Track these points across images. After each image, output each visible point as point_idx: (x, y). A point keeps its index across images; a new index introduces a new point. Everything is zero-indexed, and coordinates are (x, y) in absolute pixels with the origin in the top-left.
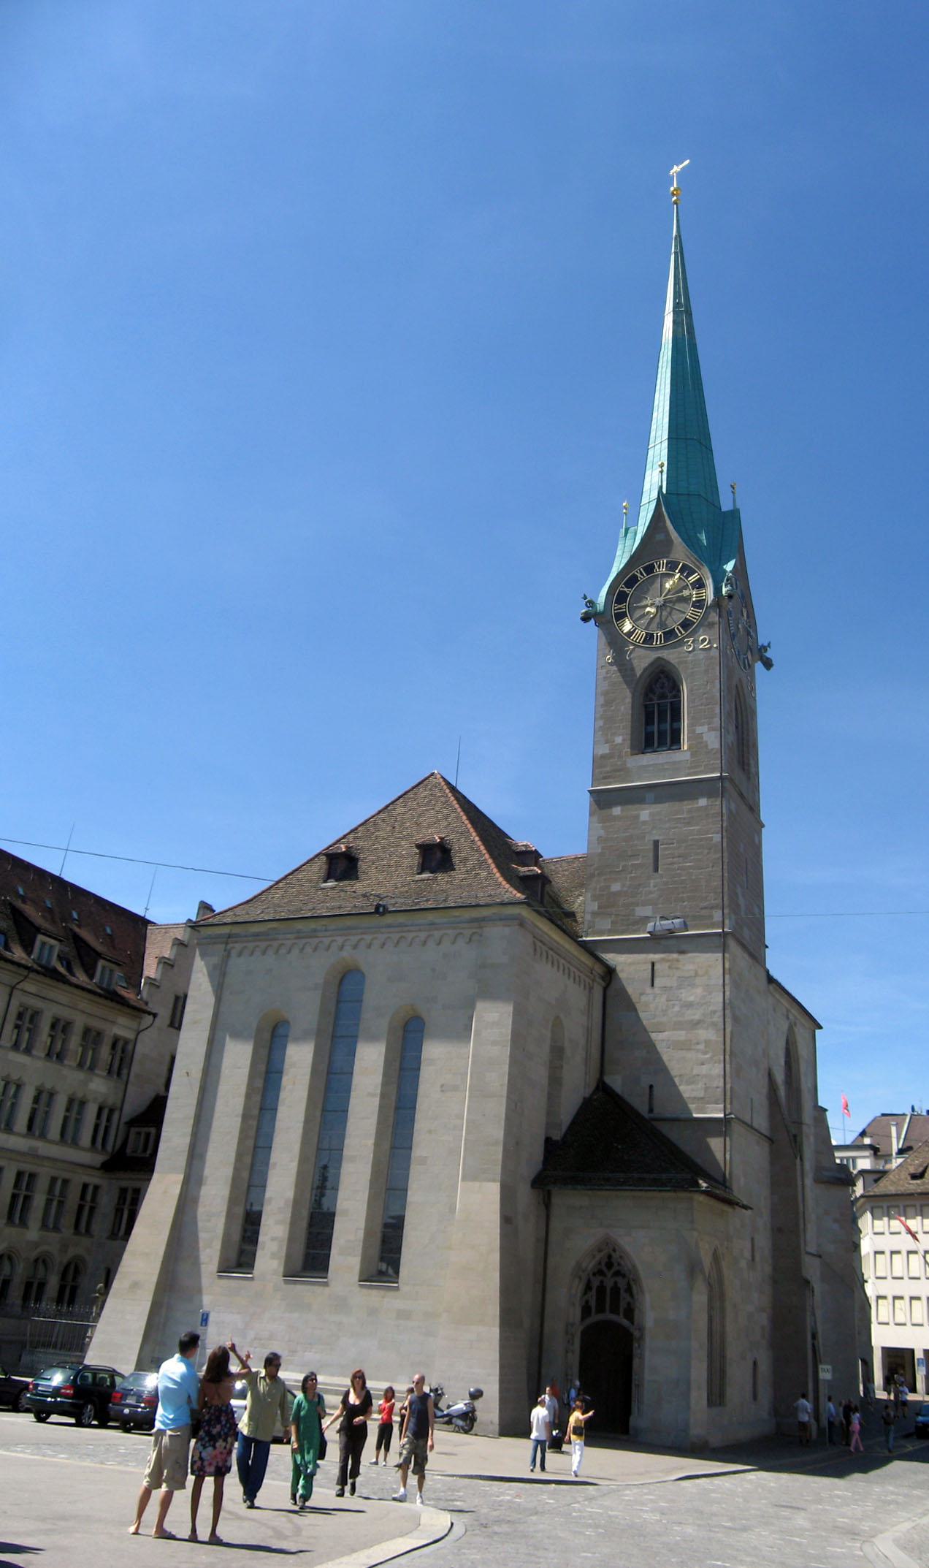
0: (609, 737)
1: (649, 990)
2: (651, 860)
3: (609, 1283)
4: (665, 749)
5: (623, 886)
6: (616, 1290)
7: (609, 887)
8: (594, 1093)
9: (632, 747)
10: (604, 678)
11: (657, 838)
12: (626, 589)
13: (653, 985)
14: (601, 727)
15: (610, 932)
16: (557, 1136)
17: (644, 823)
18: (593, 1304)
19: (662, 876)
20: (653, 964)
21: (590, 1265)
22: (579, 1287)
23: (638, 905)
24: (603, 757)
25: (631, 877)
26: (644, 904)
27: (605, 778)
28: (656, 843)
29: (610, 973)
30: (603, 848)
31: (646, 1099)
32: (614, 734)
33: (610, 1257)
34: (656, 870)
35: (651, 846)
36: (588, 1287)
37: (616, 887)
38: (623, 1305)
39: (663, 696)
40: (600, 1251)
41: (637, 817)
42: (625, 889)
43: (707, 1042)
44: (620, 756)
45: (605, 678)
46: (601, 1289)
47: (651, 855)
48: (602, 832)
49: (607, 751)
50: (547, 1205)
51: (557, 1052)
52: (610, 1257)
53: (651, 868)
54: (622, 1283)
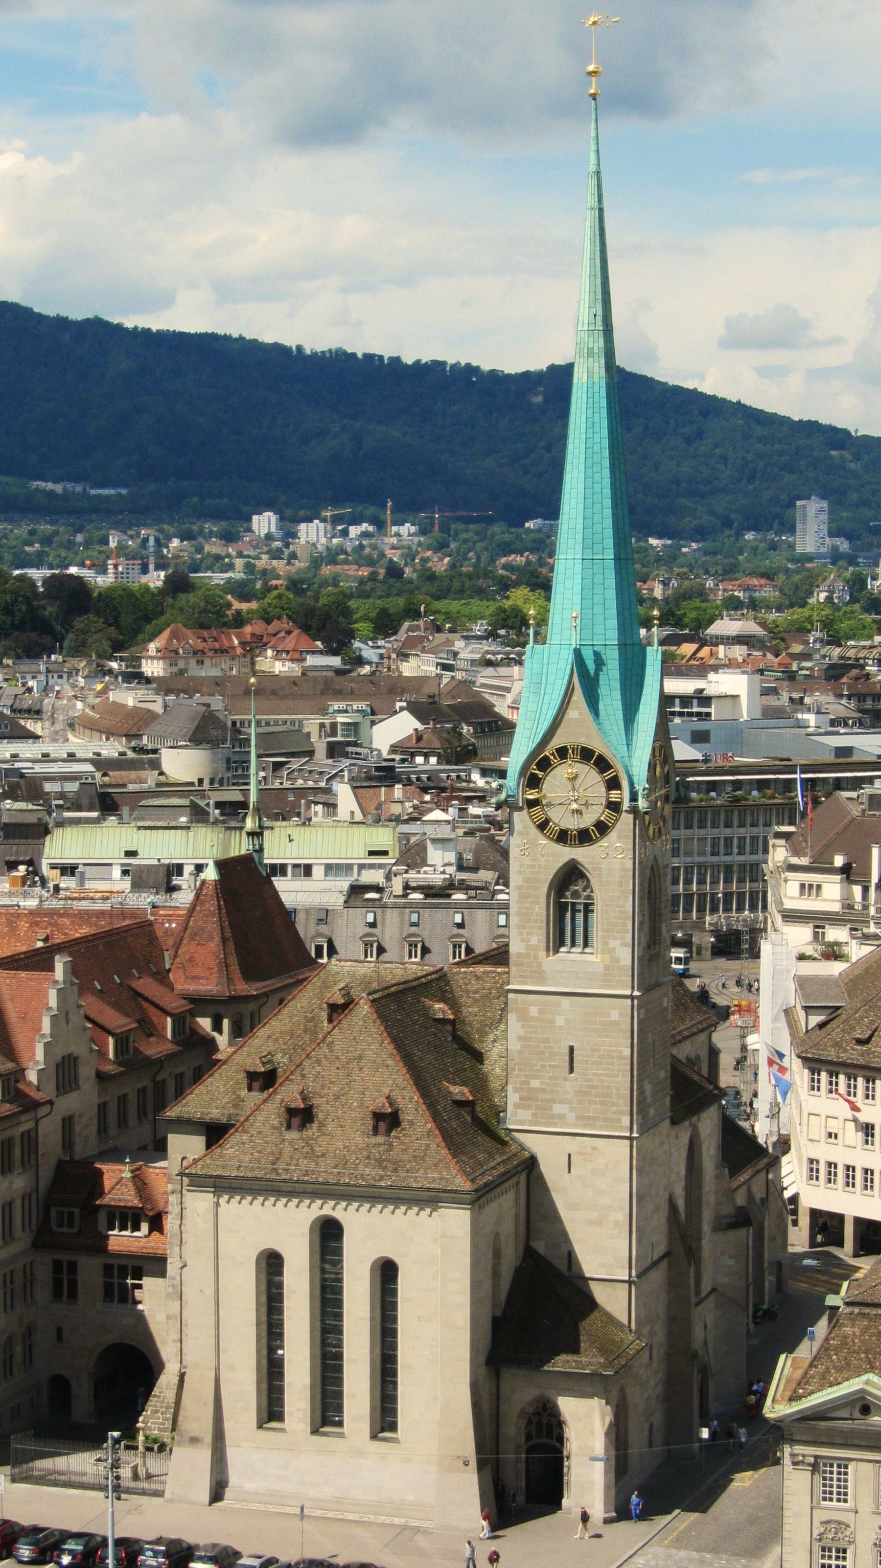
0: (525, 936)
1: (566, 1175)
2: (567, 1064)
3: (545, 1420)
4: (579, 950)
5: (542, 1083)
6: (549, 1425)
7: (527, 1083)
8: (521, 1263)
9: (548, 950)
10: (519, 871)
11: (572, 1044)
12: (537, 772)
13: (569, 1172)
14: (516, 925)
15: (531, 1123)
16: (499, 1313)
17: (560, 1027)
18: (534, 1432)
19: (576, 1080)
20: (570, 1155)
21: (531, 1410)
22: (523, 1423)
23: (554, 1101)
24: (519, 955)
25: (550, 1078)
26: (561, 1102)
27: (520, 976)
28: (572, 1049)
29: (531, 1163)
30: (522, 1046)
31: (566, 1261)
32: (529, 933)
33: (545, 1404)
34: (571, 1070)
35: (567, 1051)
36: (529, 1423)
37: (535, 1084)
38: (555, 1434)
39: (576, 895)
40: (538, 1401)
41: (553, 1021)
42: (544, 1086)
43: (616, 1223)
44: (536, 957)
45: (520, 872)
46: (539, 1423)
47: (567, 1058)
48: (522, 1032)
49: (523, 951)
50: (497, 1374)
51: (497, 1253)
52: (545, 1404)
53: (567, 1069)
54: (554, 1421)
